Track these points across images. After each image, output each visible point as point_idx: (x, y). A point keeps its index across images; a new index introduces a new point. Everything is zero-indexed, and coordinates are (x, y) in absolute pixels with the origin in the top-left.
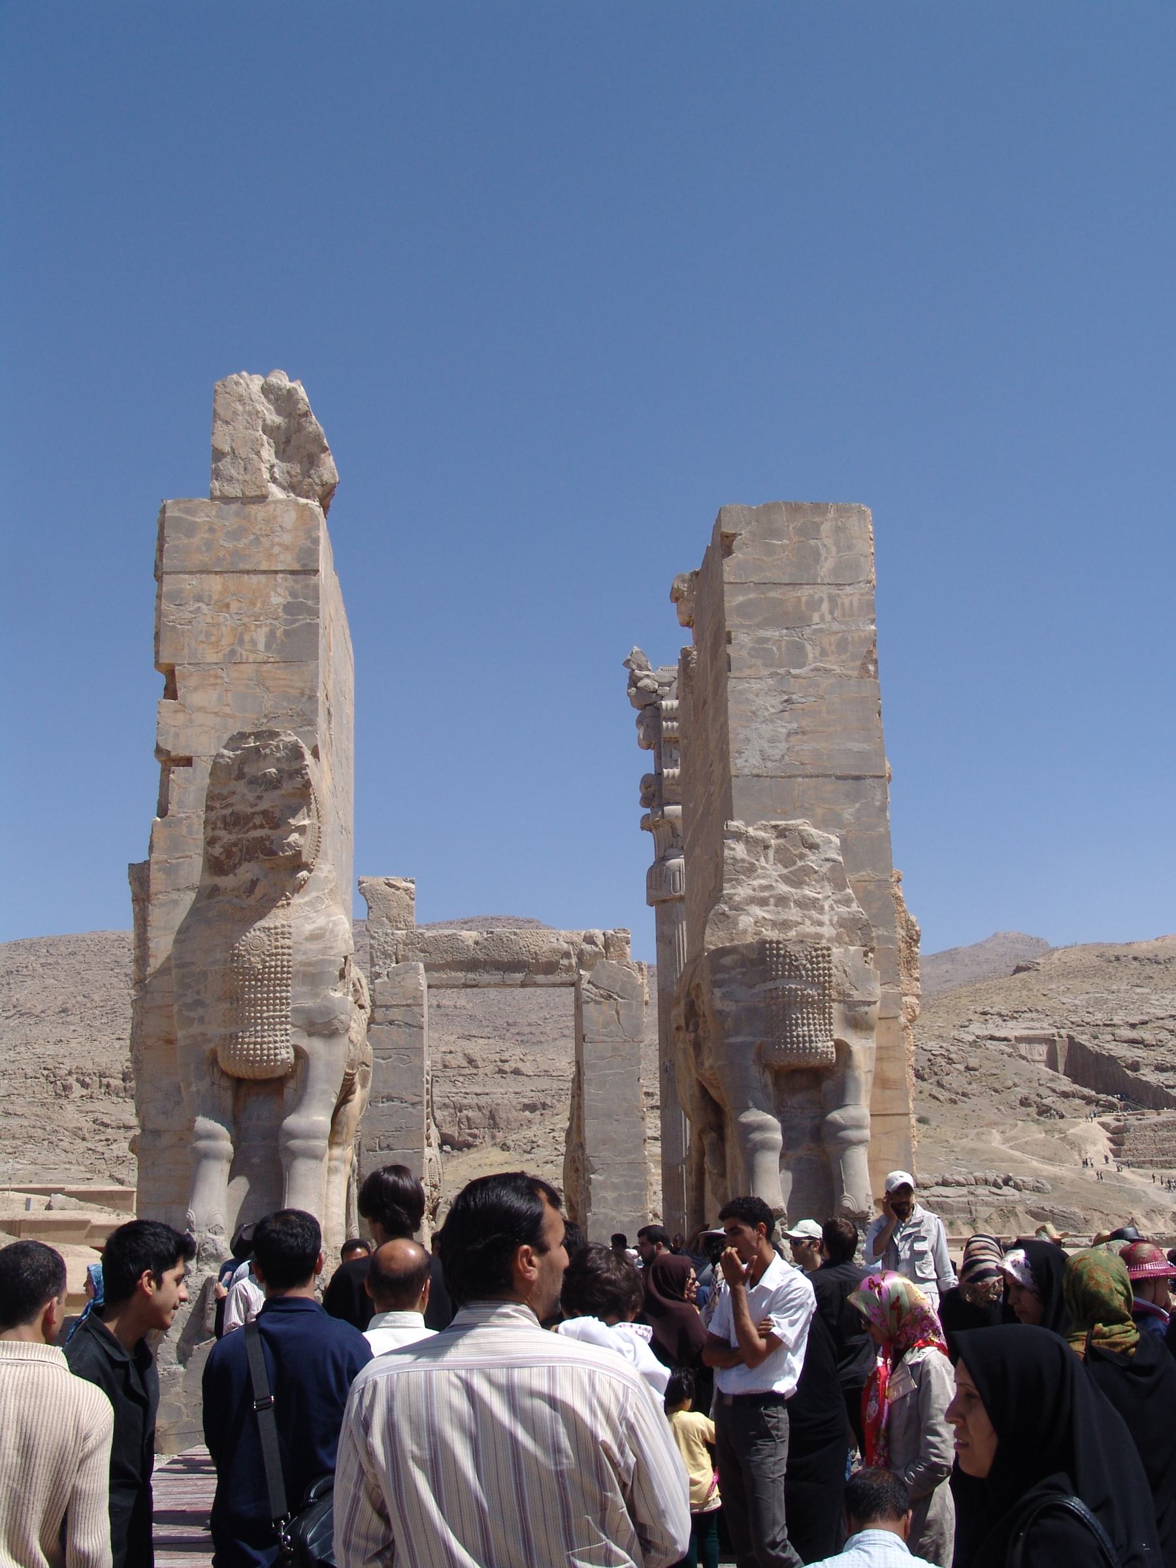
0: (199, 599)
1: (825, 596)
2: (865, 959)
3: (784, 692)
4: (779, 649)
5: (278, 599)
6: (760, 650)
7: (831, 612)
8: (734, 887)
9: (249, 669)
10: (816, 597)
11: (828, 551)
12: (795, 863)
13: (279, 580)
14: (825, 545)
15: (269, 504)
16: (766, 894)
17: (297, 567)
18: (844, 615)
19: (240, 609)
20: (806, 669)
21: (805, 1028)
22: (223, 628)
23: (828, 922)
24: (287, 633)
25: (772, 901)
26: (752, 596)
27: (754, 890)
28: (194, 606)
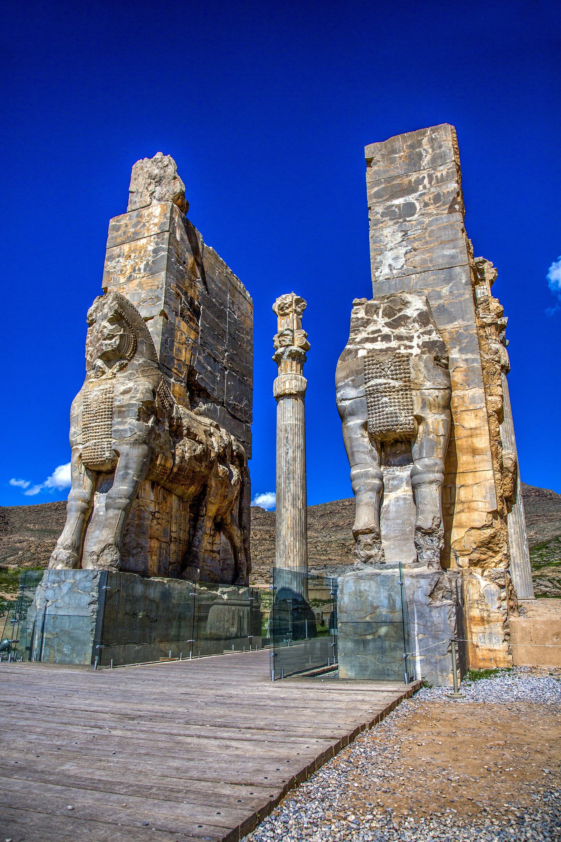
0: (119, 256)
1: (426, 175)
2: (438, 362)
3: (403, 231)
4: (399, 209)
5: (150, 248)
6: (389, 213)
7: (430, 183)
8: (356, 334)
9: (136, 282)
10: (421, 177)
11: (427, 152)
12: (396, 314)
13: (152, 239)
14: (424, 150)
15: (149, 208)
16: (376, 335)
17: (159, 231)
18: (438, 182)
19: (135, 256)
20: (416, 216)
21: (392, 409)
22: (128, 267)
23: (416, 346)
24: (153, 262)
25: (379, 339)
26: (383, 186)
27: (368, 334)
28: (117, 260)
